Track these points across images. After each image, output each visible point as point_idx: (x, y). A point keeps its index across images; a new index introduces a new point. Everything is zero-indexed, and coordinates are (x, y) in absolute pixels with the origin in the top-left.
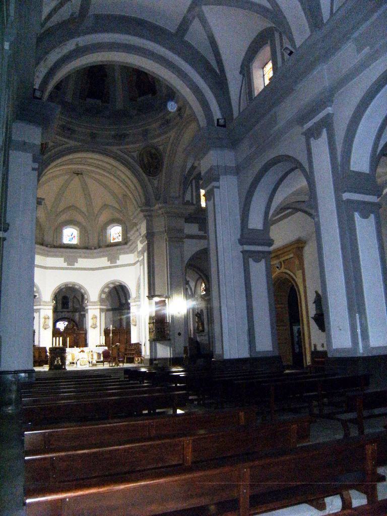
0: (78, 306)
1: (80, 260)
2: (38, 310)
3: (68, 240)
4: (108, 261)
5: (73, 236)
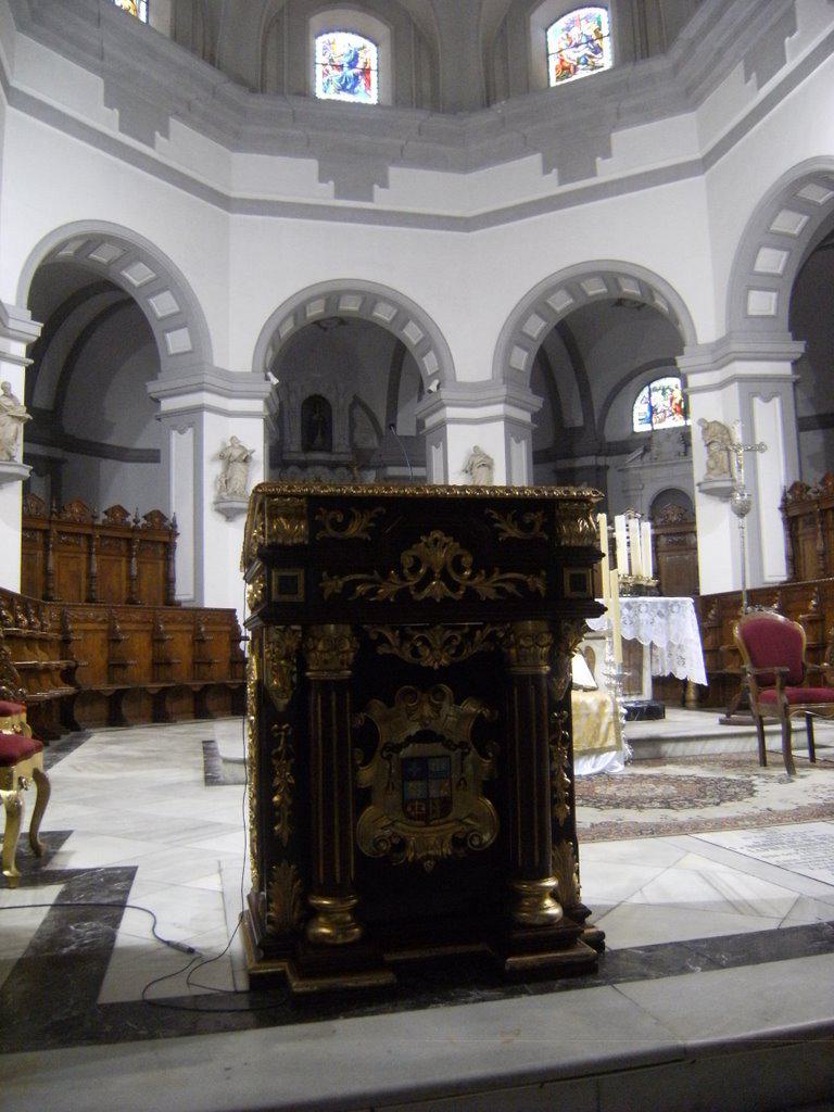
0: (373, 442)
1: (394, 172)
2: (191, 418)
3: (336, 84)
4: (546, 171)
5: (360, 65)
